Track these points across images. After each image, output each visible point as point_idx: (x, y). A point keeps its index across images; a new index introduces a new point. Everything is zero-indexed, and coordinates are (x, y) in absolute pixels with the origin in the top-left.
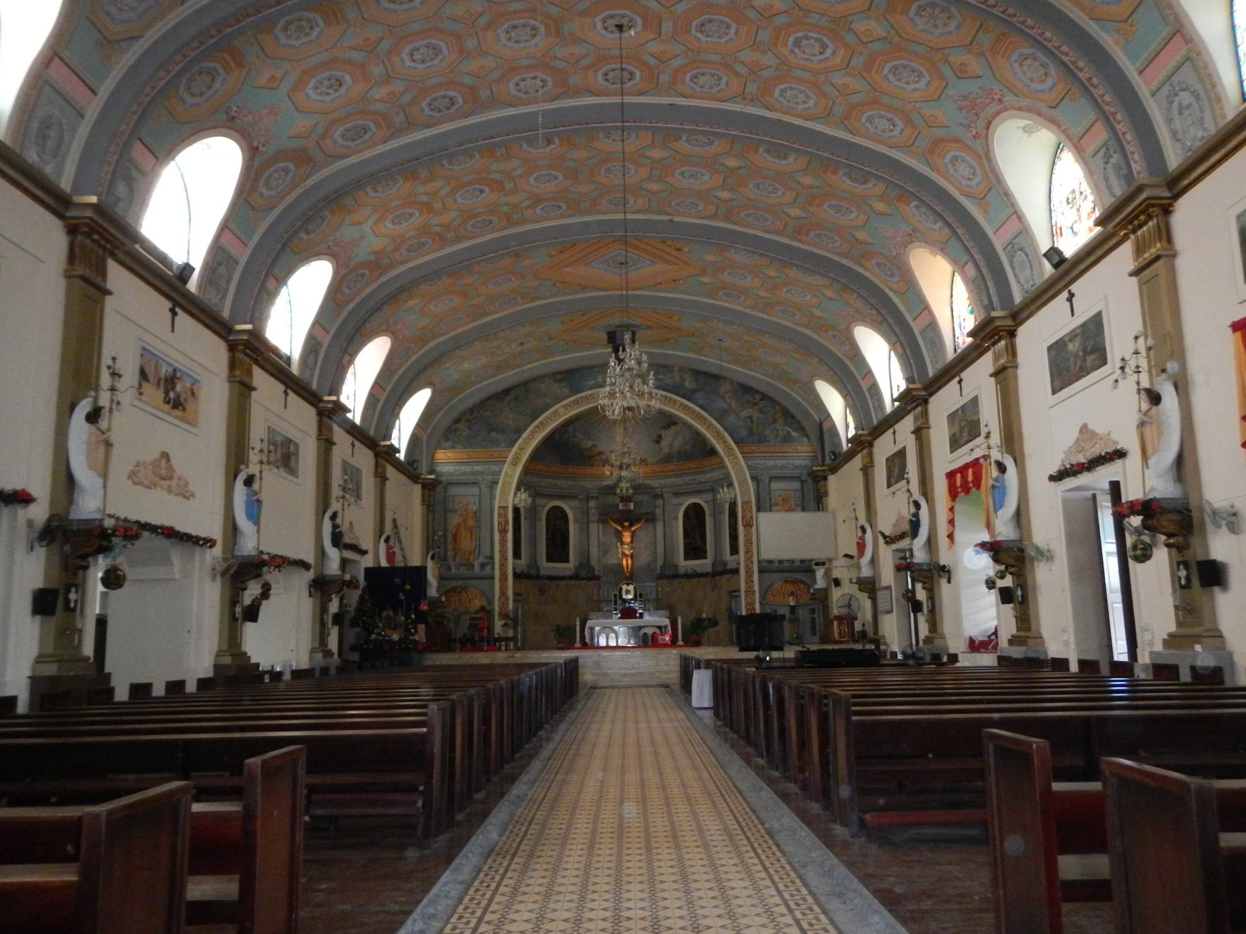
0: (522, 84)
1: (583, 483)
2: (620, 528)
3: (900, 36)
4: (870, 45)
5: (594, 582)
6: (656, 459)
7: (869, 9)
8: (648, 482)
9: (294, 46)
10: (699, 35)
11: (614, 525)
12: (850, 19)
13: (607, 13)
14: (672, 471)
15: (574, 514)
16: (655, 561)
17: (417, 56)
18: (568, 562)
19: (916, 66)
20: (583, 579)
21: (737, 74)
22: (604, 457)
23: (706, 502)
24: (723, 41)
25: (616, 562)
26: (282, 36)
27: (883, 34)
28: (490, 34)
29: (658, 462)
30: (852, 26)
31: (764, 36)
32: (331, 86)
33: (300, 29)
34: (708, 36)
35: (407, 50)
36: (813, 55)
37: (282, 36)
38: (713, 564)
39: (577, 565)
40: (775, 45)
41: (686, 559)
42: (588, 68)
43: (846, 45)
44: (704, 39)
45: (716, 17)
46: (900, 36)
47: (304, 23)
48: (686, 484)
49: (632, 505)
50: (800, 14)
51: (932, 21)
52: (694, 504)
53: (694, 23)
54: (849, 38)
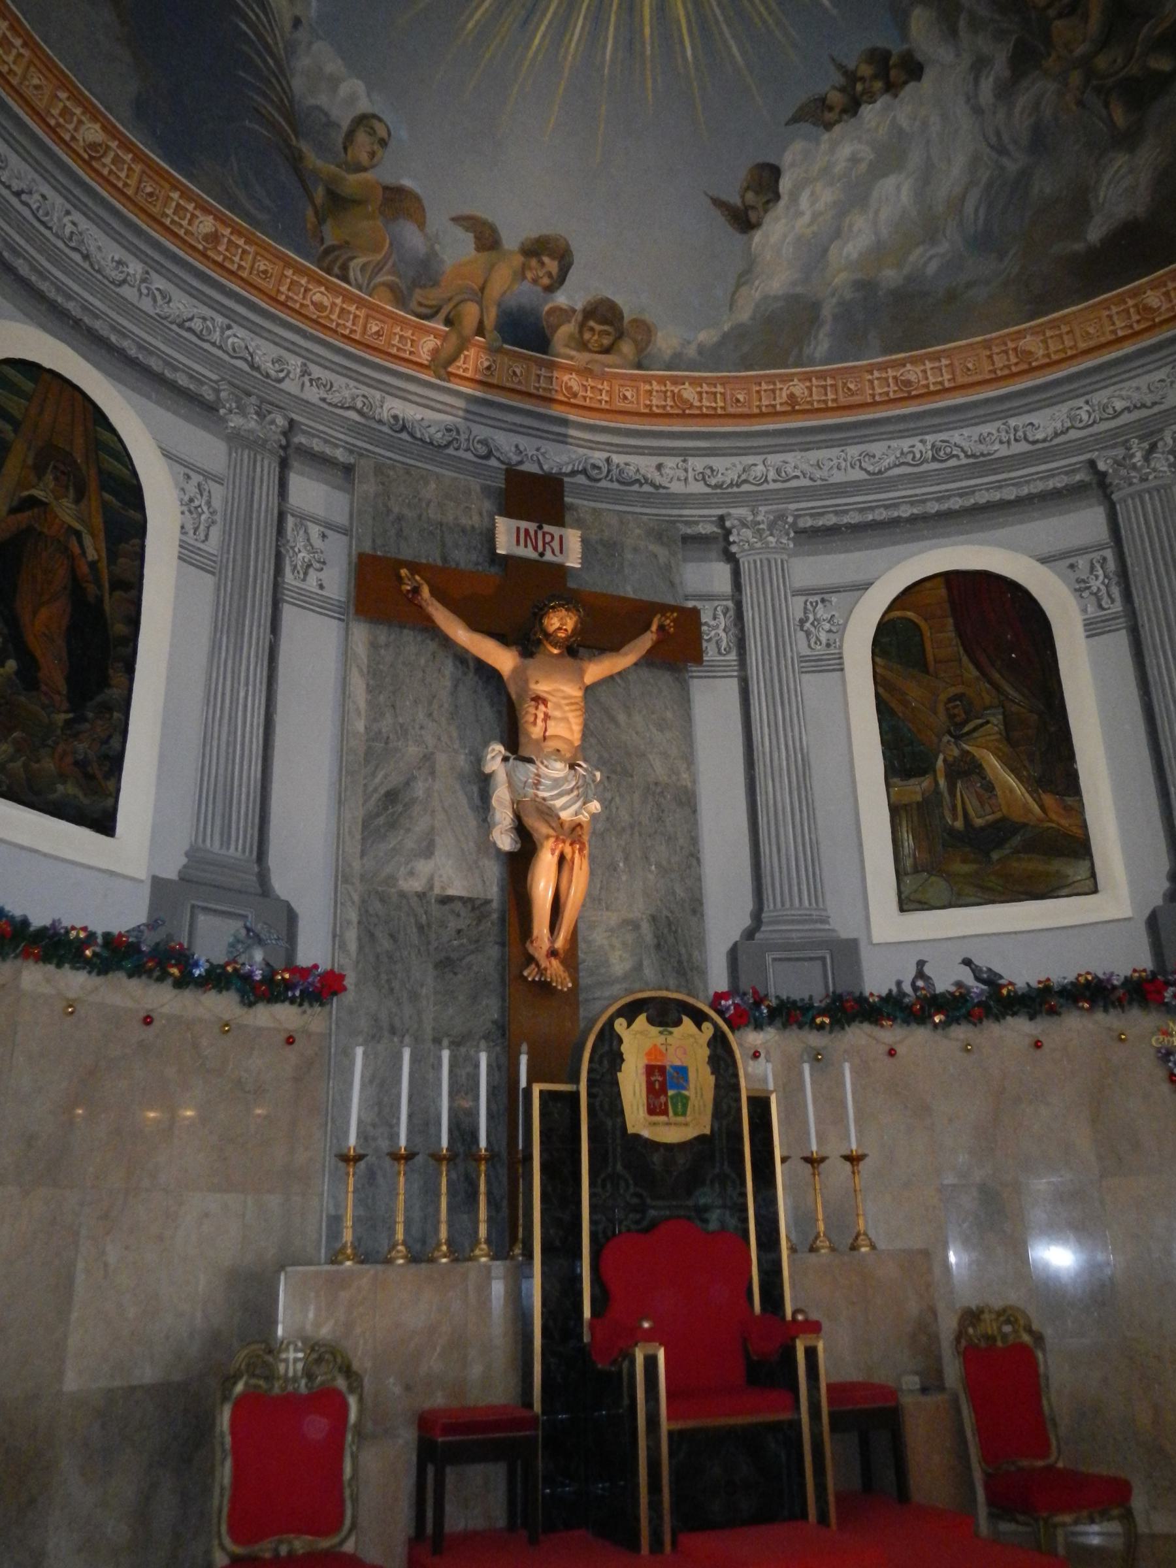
1: (265, 353)
2: (503, 660)
5: (285, 1015)
6: (707, 337)
8: (644, 465)
11: (462, 635)
14: (793, 407)
15: (189, 506)
16: (696, 905)
18: (105, 824)
20: (217, 979)
22: (412, 237)
23: (1044, 561)
25: (457, 889)
29: (710, 358)
38: (1153, 923)
39: (170, 872)
41: (906, 904)
48: (878, 481)
49: (573, 539)
52: (952, 579)
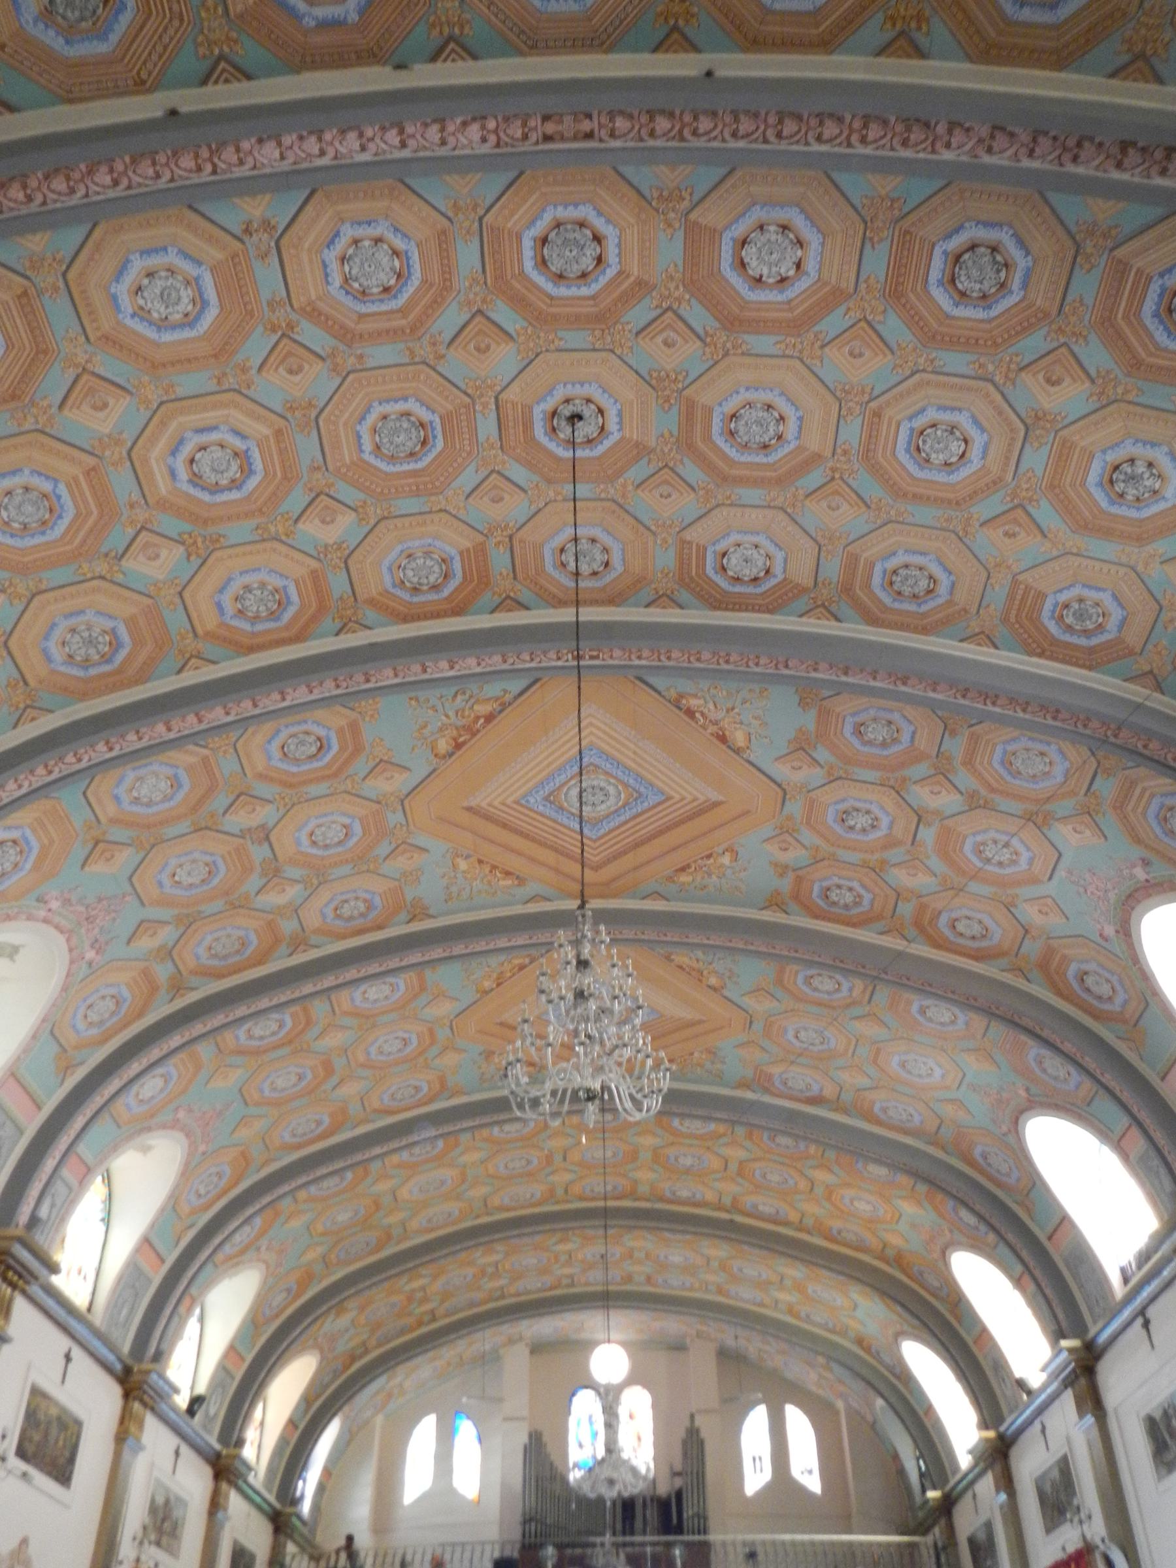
0: (788, 270)
3: (102, 578)
4: (130, 531)
7: (180, 594)
9: (1115, 597)
10: (424, 415)
12: (195, 561)
13: (600, 449)
17: (956, 447)
19: (29, 542)
21: (313, 314)
24: (378, 410)
26: (1112, 624)
27: (127, 563)
28: (814, 442)
30: (182, 549)
31: (307, 448)
32: (1133, 478)
33: (1081, 616)
34: (407, 414)
35: (964, 472)
36: (203, 448)
37: (1112, 624)
40: (278, 433)
42: (642, 287)
43: (163, 505)
44: (412, 405)
45: (406, 467)
46: (102, 578)
47: (1069, 620)
50: (272, 529)
51: (86, 634)
53: (440, 444)
54: (171, 525)
